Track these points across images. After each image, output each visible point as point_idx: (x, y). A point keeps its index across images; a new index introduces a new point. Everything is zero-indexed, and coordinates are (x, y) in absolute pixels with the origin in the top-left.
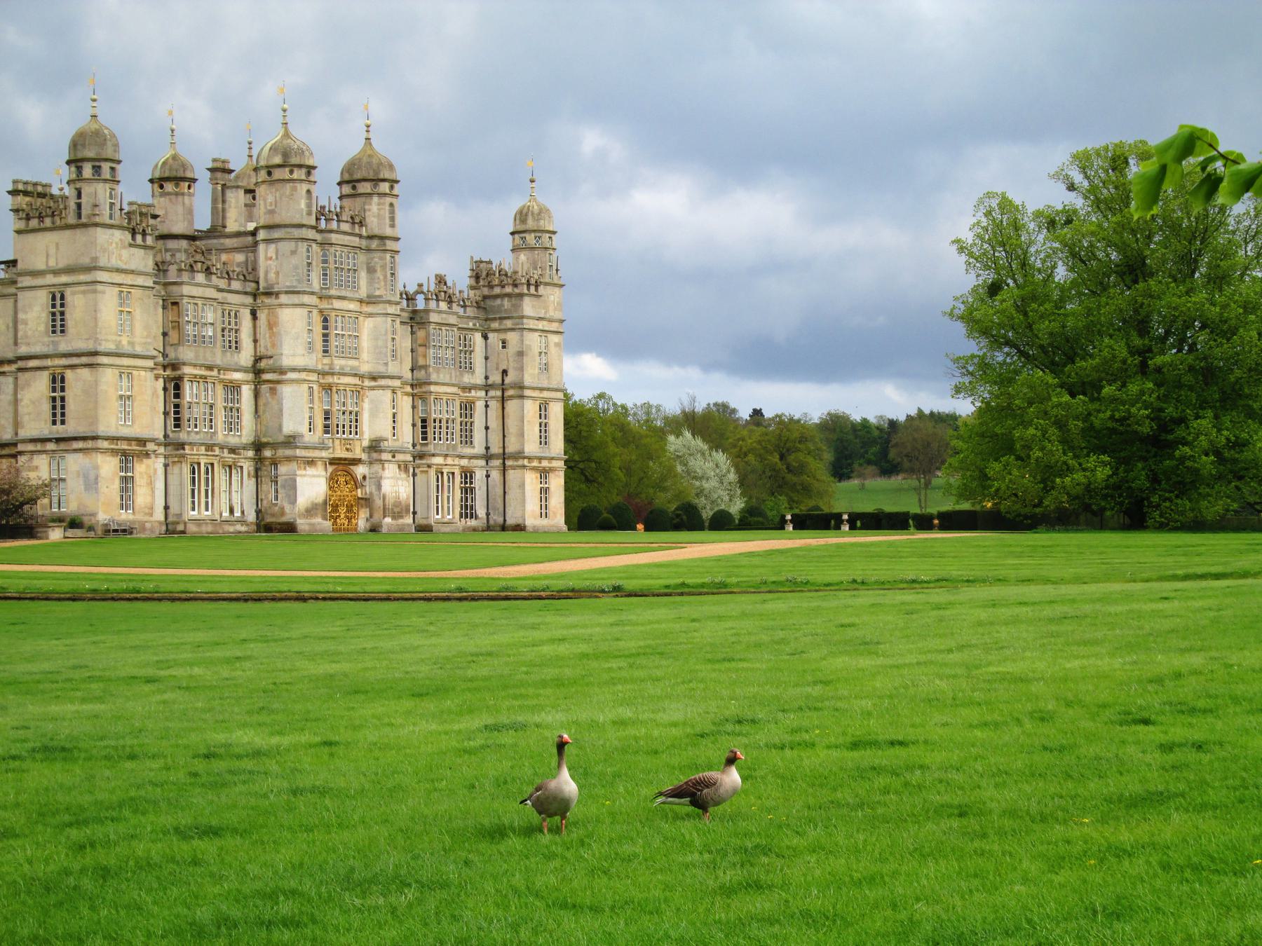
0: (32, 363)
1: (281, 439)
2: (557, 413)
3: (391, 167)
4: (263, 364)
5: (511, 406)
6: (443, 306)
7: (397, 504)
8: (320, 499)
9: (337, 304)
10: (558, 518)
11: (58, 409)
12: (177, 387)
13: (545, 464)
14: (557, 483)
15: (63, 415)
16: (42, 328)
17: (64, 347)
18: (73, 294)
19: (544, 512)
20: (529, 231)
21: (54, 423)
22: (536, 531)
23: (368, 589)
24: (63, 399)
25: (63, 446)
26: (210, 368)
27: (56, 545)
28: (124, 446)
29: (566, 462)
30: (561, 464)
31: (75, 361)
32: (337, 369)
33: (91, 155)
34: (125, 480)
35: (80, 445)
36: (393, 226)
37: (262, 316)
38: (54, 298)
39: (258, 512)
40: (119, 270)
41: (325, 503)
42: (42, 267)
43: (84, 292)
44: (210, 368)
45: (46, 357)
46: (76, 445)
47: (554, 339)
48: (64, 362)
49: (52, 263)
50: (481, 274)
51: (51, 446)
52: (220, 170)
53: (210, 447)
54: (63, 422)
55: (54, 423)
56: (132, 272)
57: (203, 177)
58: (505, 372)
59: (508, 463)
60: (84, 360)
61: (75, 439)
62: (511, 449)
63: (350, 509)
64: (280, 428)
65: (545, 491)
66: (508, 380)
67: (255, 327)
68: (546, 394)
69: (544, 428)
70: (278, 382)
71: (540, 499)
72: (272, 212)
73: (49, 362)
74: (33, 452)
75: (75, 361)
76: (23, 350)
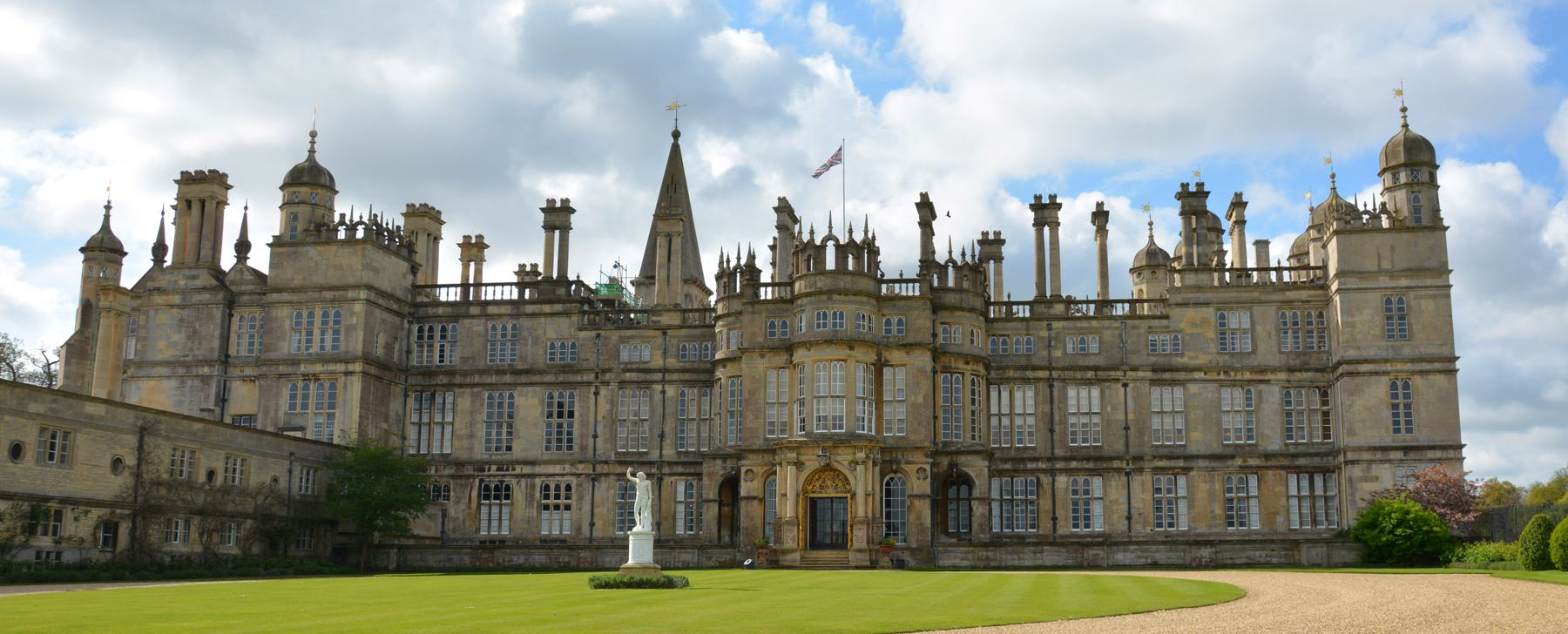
0: (1364, 368)
11: (1402, 413)
15: (1409, 422)
16: (1377, 331)
17: (1407, 351)
18: (1418, 298)
21: (1397, 431)
25: (1412, 455)
31: (1425, 366)
35: (1438, 454)
38: (1389, 301)
42: (1375, 269)
43: (1434, 297)
45: (1386, 361)
46: (1430, 454)
48: (1409, 366)
49: (1386, 265)
51: (1399, 455)
54: (1409, 431)
55: (1397, 431)
60: (1437, 366)
61: (1432, 448)
73: (1388, 367)
74: (1370, 462)
75: (1425, 366)
76: (1352, 354)
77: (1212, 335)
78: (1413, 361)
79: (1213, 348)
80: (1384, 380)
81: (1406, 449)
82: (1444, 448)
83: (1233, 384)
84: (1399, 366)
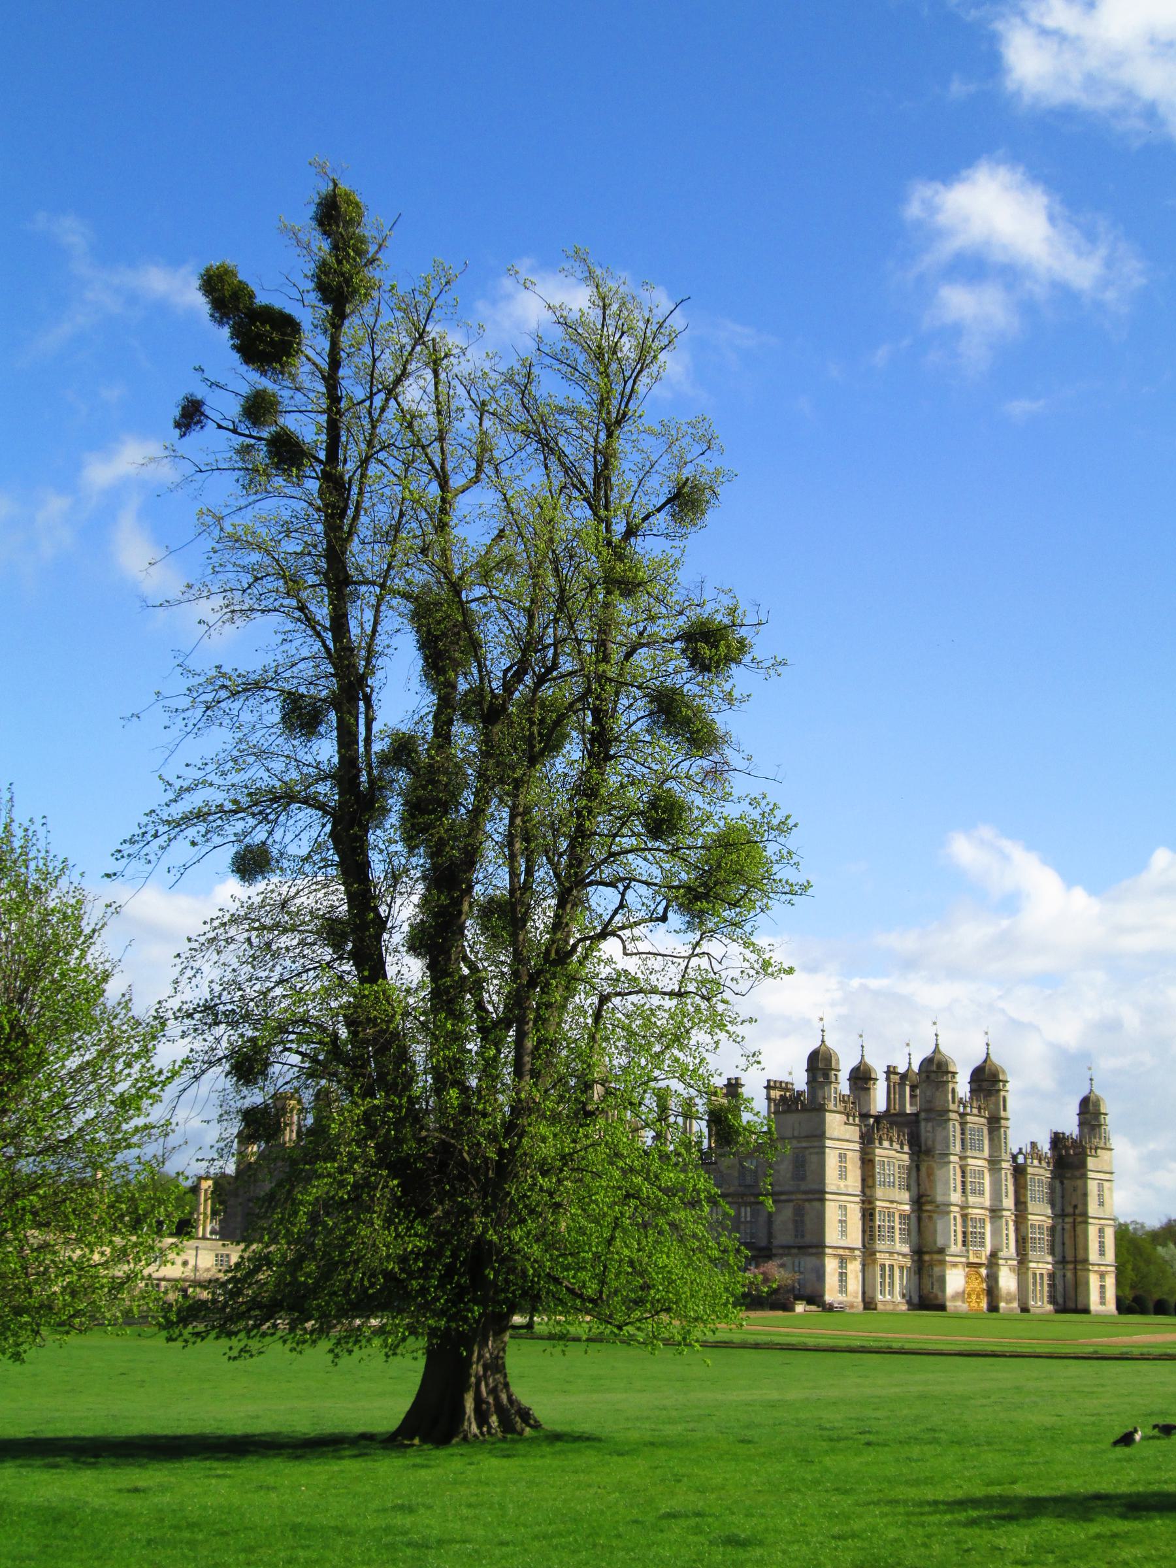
0: (783, 1197)
1: (935, 1249)
2: (1109, 1233)
3: (1004, 1072)
4: (924, 1199)
5: (1079, 1228)
6: (1036, 1162)
7: (1009, 1294)
8: (961, 1290)
9: (970, 1161)
10: (1111, 1306)
12: (872, 1215)
13: (1103, 1268)
14: (1110, 1281)
16: (789, 1175)
17: (803, 1187)
19: (1103, 1301)
20: (1090, 1112)
22: (1098, 1315)
23: (1019, 1350)
24: (803, 1222)
26: (892, 1202)
27: (800, 1314)
28: (841, 1252)
29: (1117, 1268)
30: (1113, 1269)
31: (811, 1196)
32: (971, 1204)
33: (820, 1064)
34: (841, 1274)
36: (1005, 1110)
37: (923, 1169)
39: (920, 1297)
40: (839, 1140)
41: (964, 1292)
44: (892, 1202)
45: (791, 1193)
46: (811, 1250)
47: (1106, 1184)
48: (804, 1197)
50: (1057, 1140)
51: (795, 1251)
52: (890, 1071)
53: (891, 1253)
56: (847, 1141)
57: (881, 1076)
58: (1075, 1207)
59: (1079, 1267)
61: (810, 1247)
62: (1080, 1257)
63: (978, 1297)
64: (935, 1242)
65: (1102, 1287)
66: (1077, 1212)
67: (918, 1176)
68: (1103, 1222)
69: (1102, 1245)
70: (934, 1212)
71: (1101, 1291)
72: (929, 1102)
75: (811, 1196)
77: (736, 1174)
78: (805, 1192)
79: (736, 1183)
80: (791, 1204)
81: (799, 1248)
82: (817, 1247)
83: (746, 1204)
84: (799, 1196)
